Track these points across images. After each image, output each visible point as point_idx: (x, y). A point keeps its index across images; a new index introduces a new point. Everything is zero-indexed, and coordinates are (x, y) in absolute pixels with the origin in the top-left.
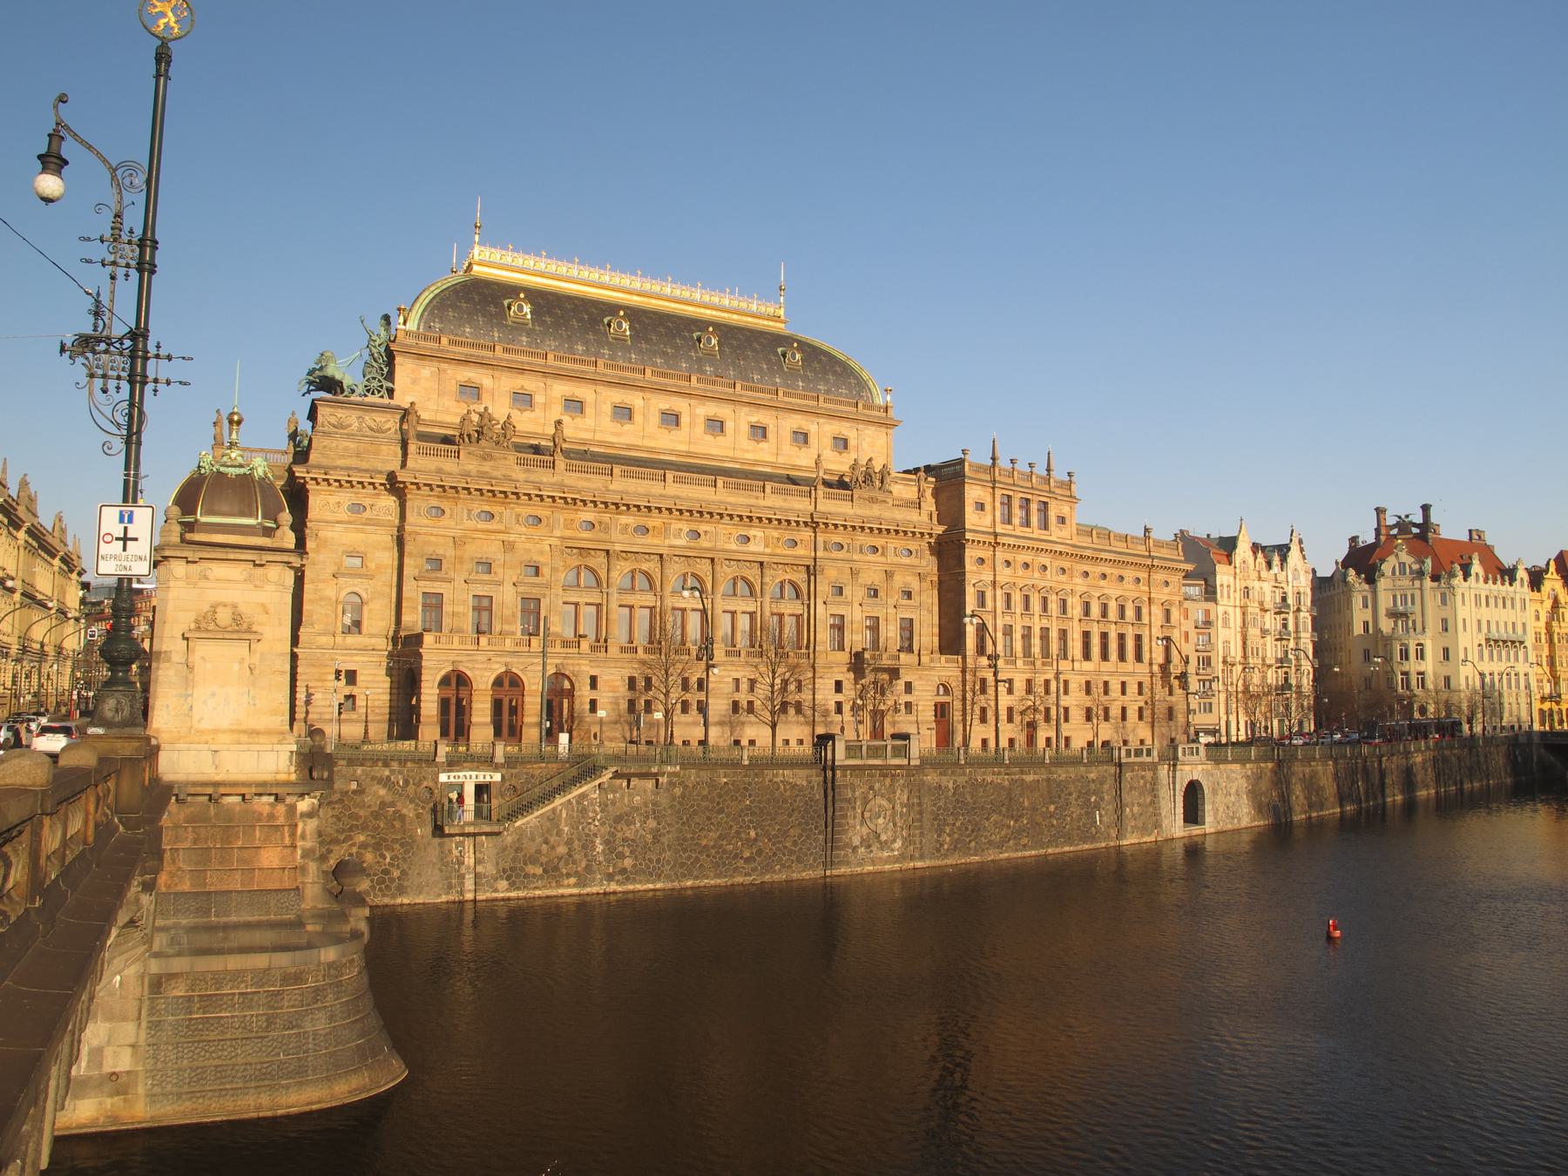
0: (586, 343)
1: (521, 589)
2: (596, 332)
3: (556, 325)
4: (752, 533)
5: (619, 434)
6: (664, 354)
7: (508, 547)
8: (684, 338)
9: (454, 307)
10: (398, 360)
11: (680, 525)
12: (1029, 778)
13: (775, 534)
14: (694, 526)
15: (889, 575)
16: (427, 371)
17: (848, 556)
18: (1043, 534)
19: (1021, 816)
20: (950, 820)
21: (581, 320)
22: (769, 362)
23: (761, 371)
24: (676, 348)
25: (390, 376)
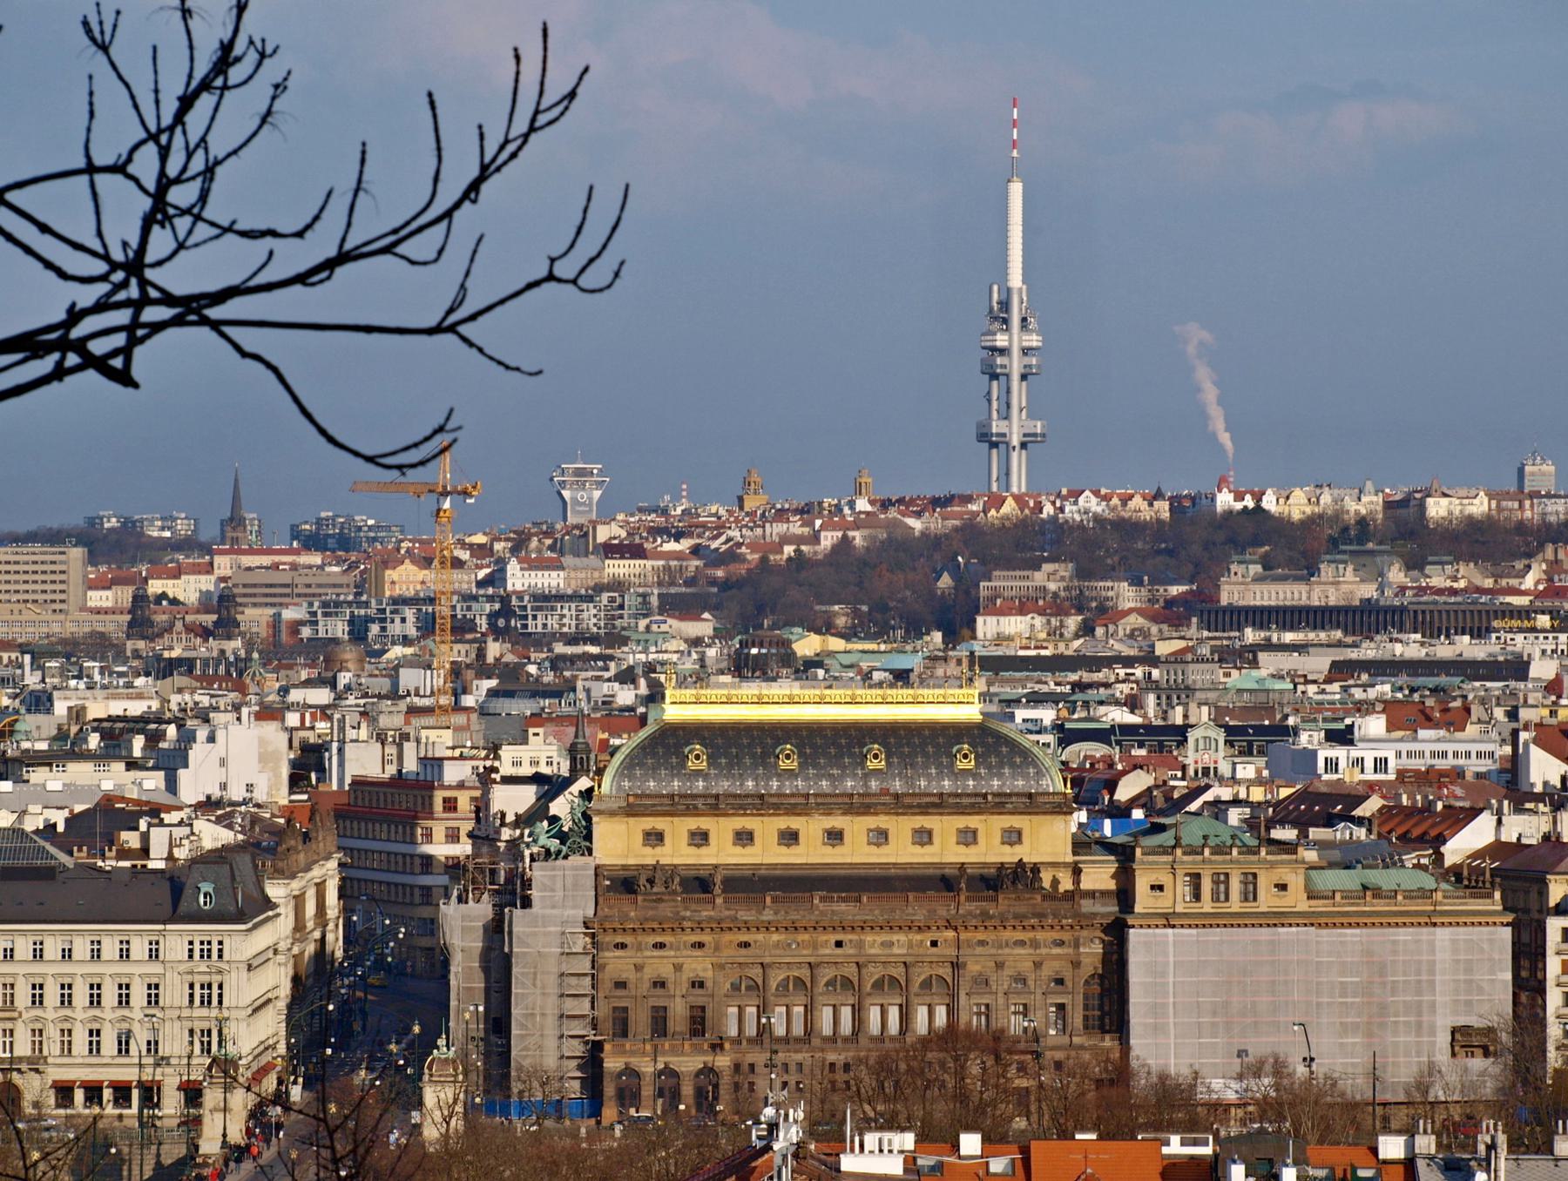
0: (756, 779)
1: (690, 999)
2: (765, 765)
3: (730, 766)
4: (895, 938)
6: (830, 777)
7: (678, 968)
8: (851, 755)
9: (641, 765)
10: (595, 819)
11: (825, 938)
13: (919, 937)
14: (839, 937)
15: (1038, 965)
17: (993, 951)
18: (1250, 907)
21: (753, 756)
22: (939, 766)
23: (929, 777)
24: (843, 768)
25: (589, 837)
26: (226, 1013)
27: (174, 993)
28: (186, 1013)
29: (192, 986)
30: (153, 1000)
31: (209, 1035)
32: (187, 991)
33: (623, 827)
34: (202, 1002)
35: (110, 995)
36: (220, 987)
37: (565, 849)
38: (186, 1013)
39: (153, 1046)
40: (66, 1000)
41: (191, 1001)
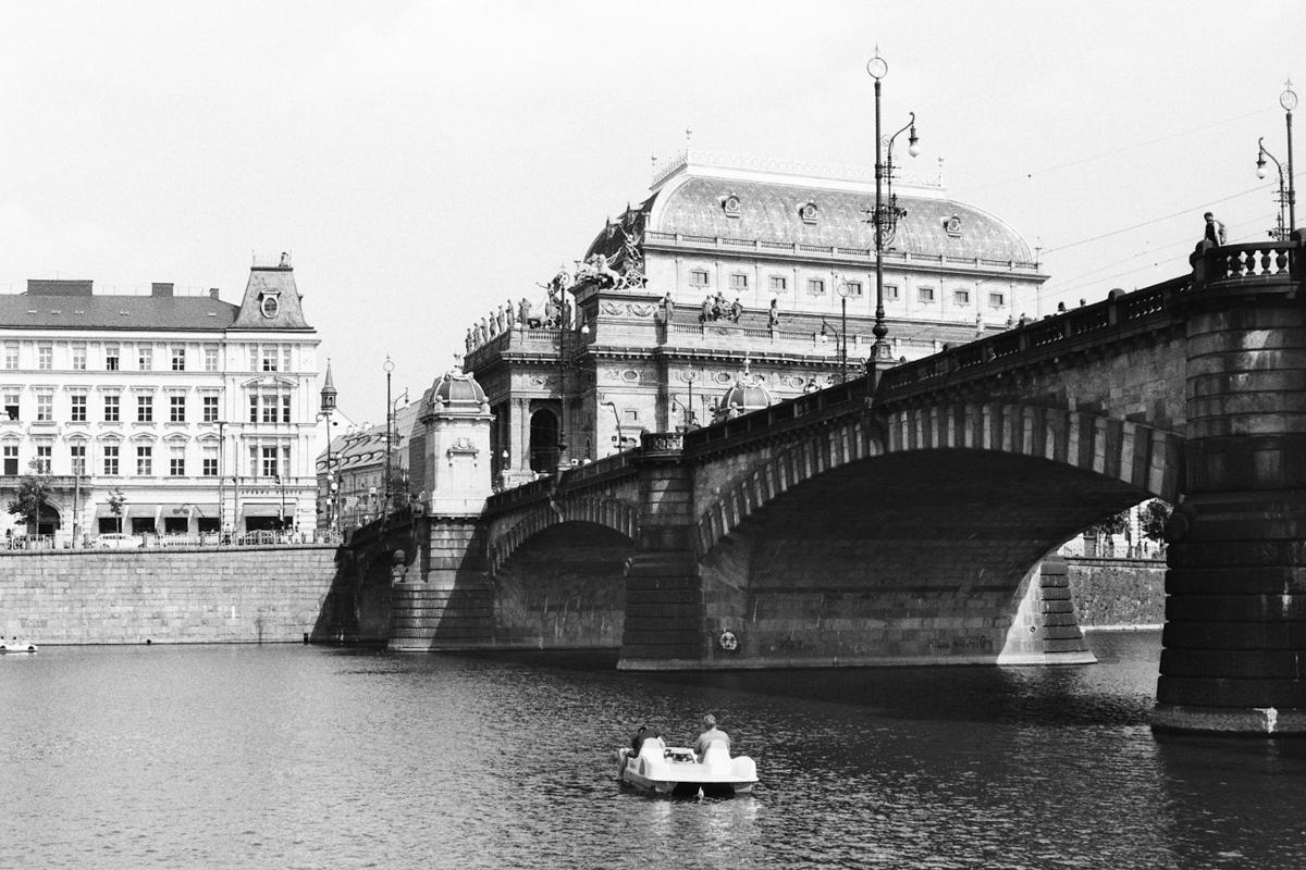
5: (815, 304)
12: (1152, 571)
16: (668, 262)
19: (1146, 599)
20: (1090, 598)
25: (643, 271)
26: (293, 430)
27: (234, 407)
28: (249, 430)
29: (254, 401)
30: (211, 414)
31: (274, 455)
32: (249, 407)
33: (673, 261)
34: (266, 419)
35: (162, 409)
36: (287, 401)
37: (624, 279)
38: (249, 430)
39: (211, 467)
40: (112, 414)
41: (254, 419)
